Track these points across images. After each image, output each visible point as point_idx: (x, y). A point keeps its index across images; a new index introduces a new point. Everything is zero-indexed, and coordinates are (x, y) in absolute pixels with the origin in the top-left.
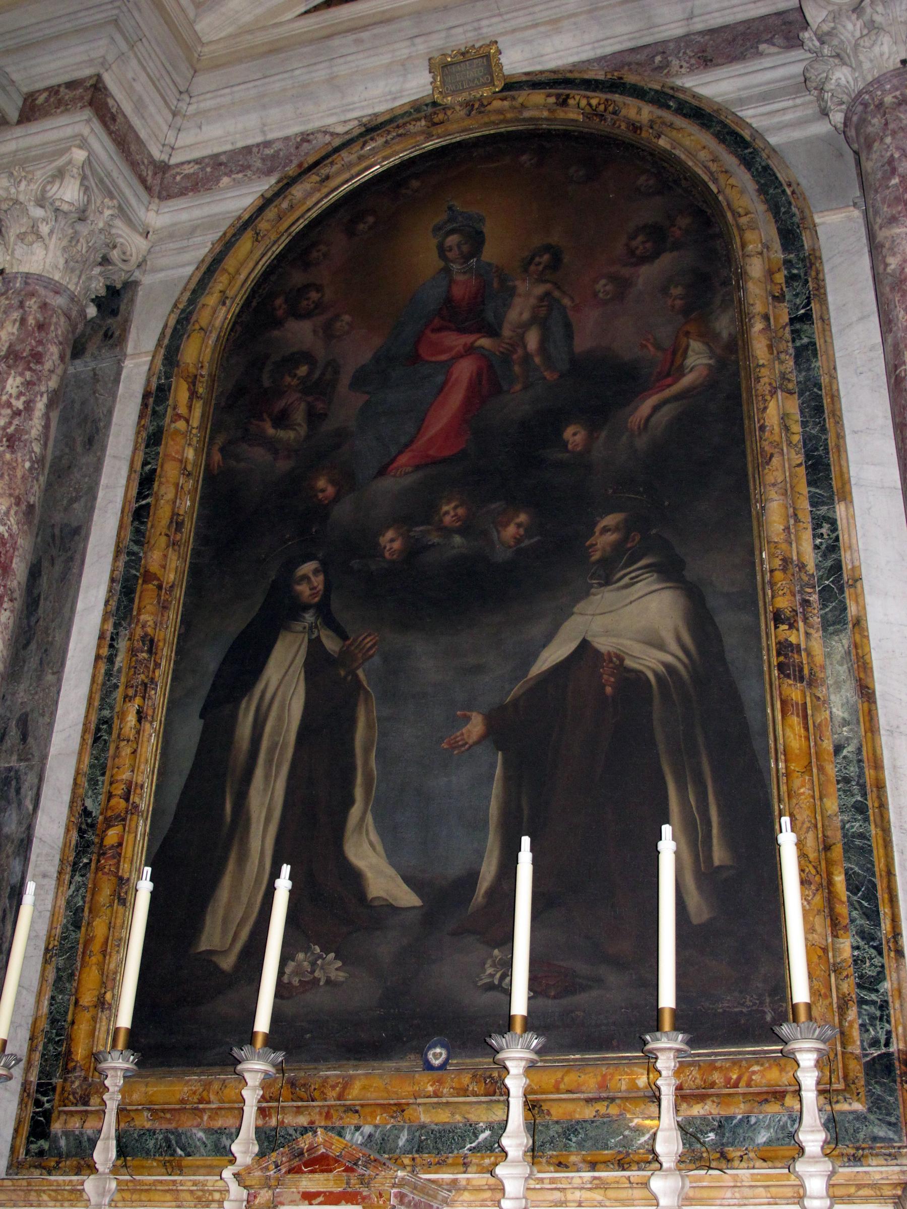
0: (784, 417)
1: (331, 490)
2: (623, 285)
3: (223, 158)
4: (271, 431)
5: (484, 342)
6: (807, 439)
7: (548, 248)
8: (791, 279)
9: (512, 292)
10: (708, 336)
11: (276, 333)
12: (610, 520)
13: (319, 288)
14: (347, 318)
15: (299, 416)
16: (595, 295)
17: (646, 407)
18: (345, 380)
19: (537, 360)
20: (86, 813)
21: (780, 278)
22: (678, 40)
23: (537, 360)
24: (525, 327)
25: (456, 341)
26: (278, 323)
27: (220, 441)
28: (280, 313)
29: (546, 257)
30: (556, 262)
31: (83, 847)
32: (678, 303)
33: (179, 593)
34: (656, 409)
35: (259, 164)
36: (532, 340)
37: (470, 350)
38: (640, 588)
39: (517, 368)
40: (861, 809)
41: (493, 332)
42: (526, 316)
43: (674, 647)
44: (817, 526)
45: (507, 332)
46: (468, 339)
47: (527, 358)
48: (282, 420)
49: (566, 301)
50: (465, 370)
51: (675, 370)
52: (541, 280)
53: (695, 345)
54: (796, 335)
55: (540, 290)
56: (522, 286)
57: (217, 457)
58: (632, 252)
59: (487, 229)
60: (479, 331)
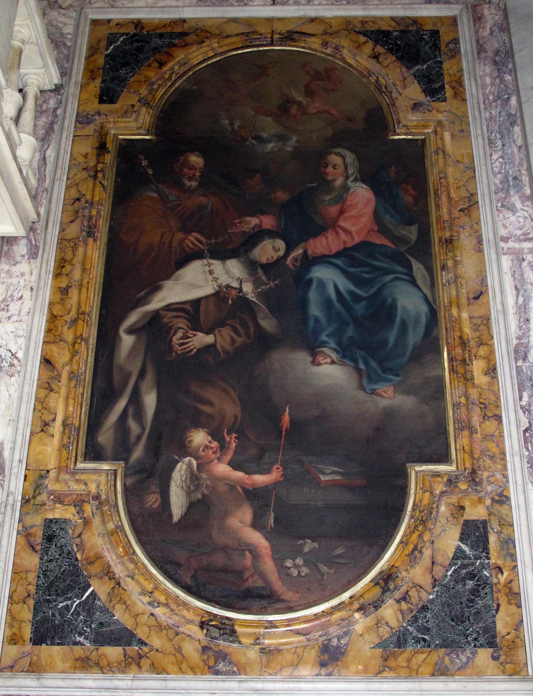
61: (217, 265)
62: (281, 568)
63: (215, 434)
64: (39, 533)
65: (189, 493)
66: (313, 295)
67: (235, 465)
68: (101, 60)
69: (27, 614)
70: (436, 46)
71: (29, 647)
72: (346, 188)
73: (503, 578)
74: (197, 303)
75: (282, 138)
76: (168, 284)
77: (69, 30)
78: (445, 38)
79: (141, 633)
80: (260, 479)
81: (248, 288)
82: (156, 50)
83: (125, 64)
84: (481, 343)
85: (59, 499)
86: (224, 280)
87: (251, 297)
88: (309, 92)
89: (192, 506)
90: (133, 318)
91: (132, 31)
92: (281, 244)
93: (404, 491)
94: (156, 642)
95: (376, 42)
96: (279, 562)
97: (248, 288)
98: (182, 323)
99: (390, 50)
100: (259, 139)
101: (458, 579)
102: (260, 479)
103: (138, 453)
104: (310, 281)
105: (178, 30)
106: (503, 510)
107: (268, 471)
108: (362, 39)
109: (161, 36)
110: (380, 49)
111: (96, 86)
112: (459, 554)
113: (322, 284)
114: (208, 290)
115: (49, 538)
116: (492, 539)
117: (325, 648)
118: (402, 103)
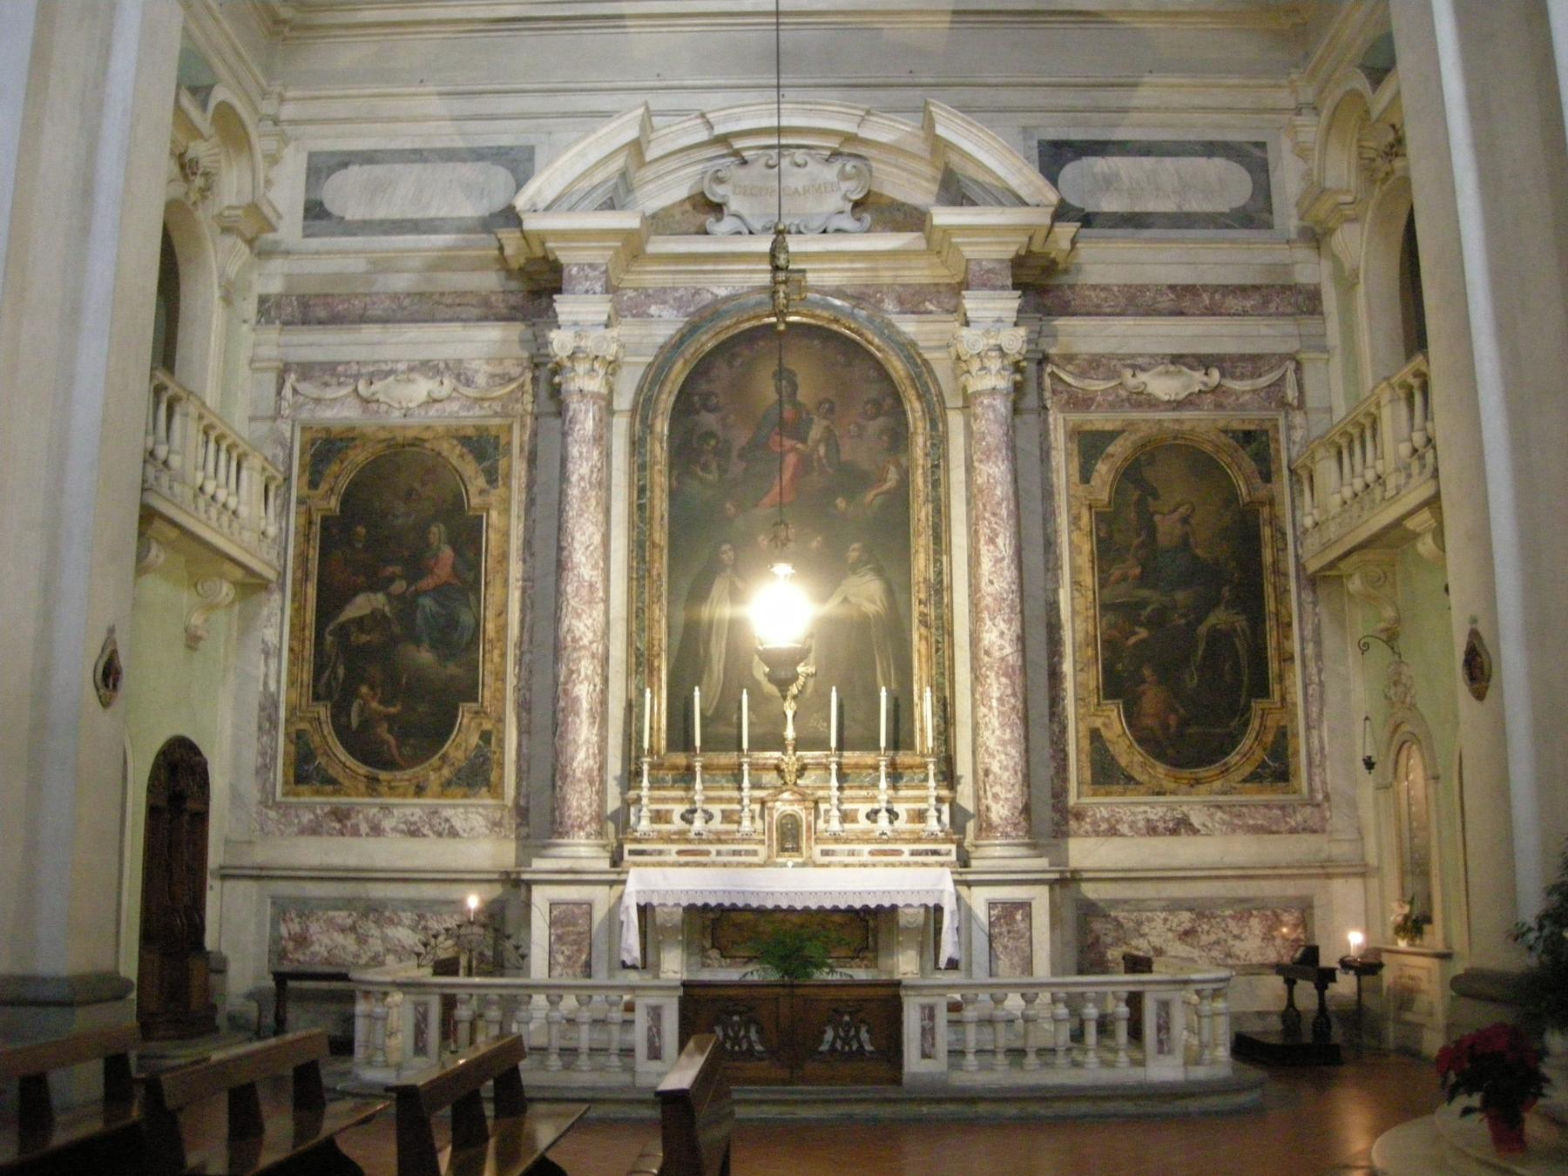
0: (927, 515)
1: (733, 510)
2: (861, 428)
3: (650, 291)
4: (700, 473)
5: (800, 446)
6: (934, 523)
7: (828, 400)
8: (933, 445)
9: (811, 421)
10: (898, 465)
11: (696, 417)
12: (856, 545)
13: (717, 396)
14: (732, 417)
15: (714, 466)
16: (849, 431)
17: (870, 496)
18: (735, 453)
19: (824, 461)
20: (638, 649)
21: (928, 444)
22: (889, 286)
23: (824, 461)
24: (819, 441)
25: (788, 443)
26: (697, 412)
27: (675, 472)
28: (697, 406)
29: (827, 406)
30: (831, 410)
31: (639, 664)
32: (886, 445)
33: (666, 551)
34: (877, 495)
35: (671, 302)
36: (822, 450)
37: (793, 449)
38: (868, 577)
39: (815, 464)
40: (943, 674)
41: (804, 441)
42: (818, 436)
43: (879, 603)
44: (935, 563)
45: (810, 443)
46: (793, 442)
47: (819, 458)
48: (705, 468)
49: (837, 433)
50: (791, 459)
51: (884, 480)
52: (825, 418)
53: (892, 469)
54: (933, 473)
55: (825, 423)
56: (816, 418)
57: (675, 483)
58: (865, 412)
59: (799, 380)
60: (797, 439)
61: (372, 596)
62: (400, 753)
63: (372, 688)
64: (294, 736)
65: (359, 716)
66: (419, 615)
67: (381, 702)
68: (308, 458)
69: (291, 772)
70: (496, 448)
71: (293, 786)
72: (439, 549)
73: (496, 756)
74: (362, 619)
75: (407, 515)
76: (348, 608)
77: (288, 435)
78: (503, 441)
79: (341, 780)
80: (392, 710)
81: (387, 609)
82: (339, 451)
83: (322, 461)
84: (499, 640)
85: (301, 719)
86: (375, 604)
87: (389, 614)
88: (424, 484)
89: (361, 724)
90: (331, 627)
91: (323, 435)
92: (404, 584)
93: (456, 717)
94: (346, 783)
95: (463, 445)
96: (399, 747)
97: (387, 609)
98: (353, 629)
99: (471, 451)
100: (395, 516)
101: (476, 757)
102: (392, 710)
103: (336, 697)
104: (417, 606)
105: (351, 435)
106: (500, 726)
107: (394, 706)
108: (455, 442)
109: (341, 440)
110: (464, 450)
111: (306, 476)
112: (478, 746)
113: (424, 606)
114: (367, 611)
115: (298, 737)
116: (493, 740)
117: (418, 786)
118: (472, 490)
